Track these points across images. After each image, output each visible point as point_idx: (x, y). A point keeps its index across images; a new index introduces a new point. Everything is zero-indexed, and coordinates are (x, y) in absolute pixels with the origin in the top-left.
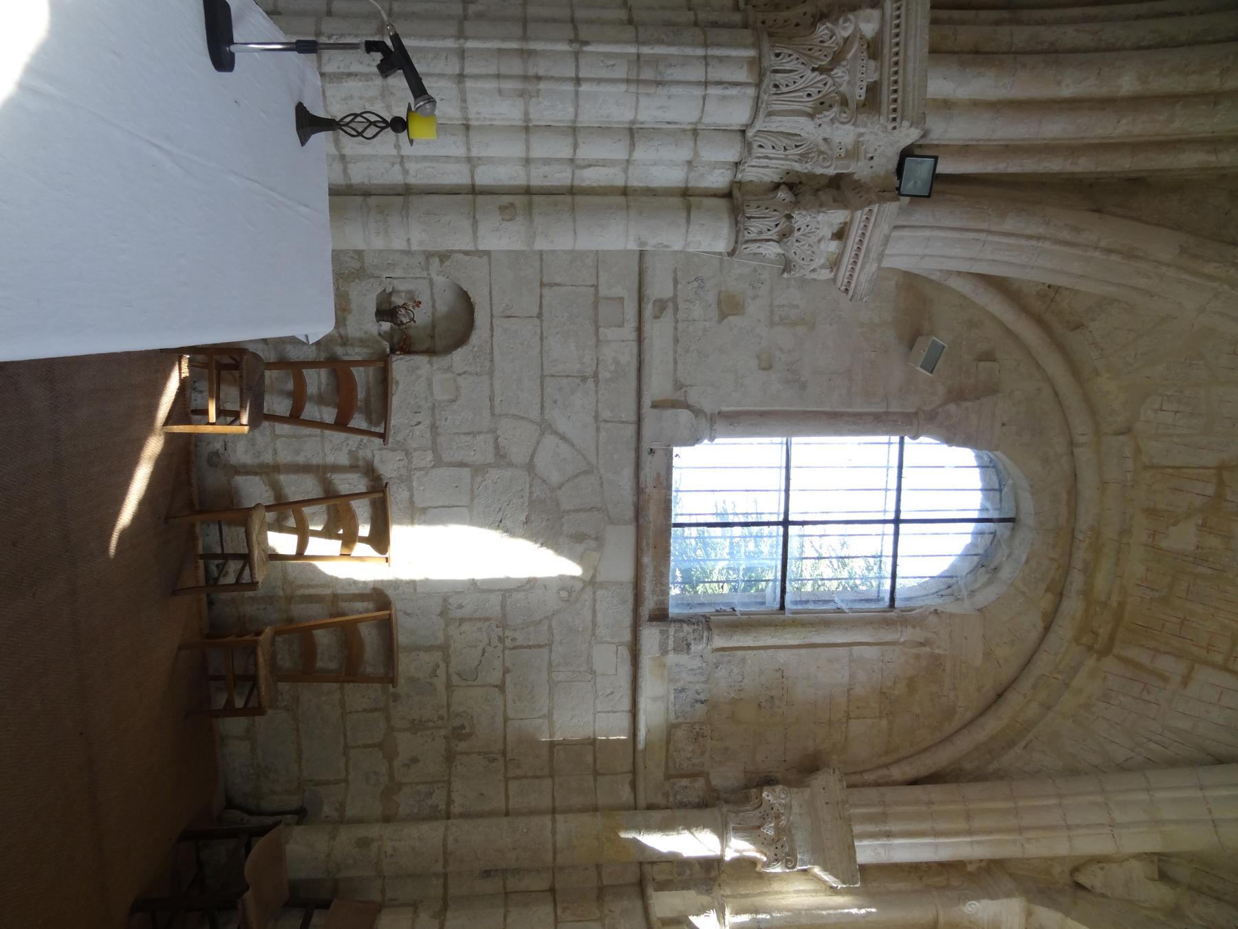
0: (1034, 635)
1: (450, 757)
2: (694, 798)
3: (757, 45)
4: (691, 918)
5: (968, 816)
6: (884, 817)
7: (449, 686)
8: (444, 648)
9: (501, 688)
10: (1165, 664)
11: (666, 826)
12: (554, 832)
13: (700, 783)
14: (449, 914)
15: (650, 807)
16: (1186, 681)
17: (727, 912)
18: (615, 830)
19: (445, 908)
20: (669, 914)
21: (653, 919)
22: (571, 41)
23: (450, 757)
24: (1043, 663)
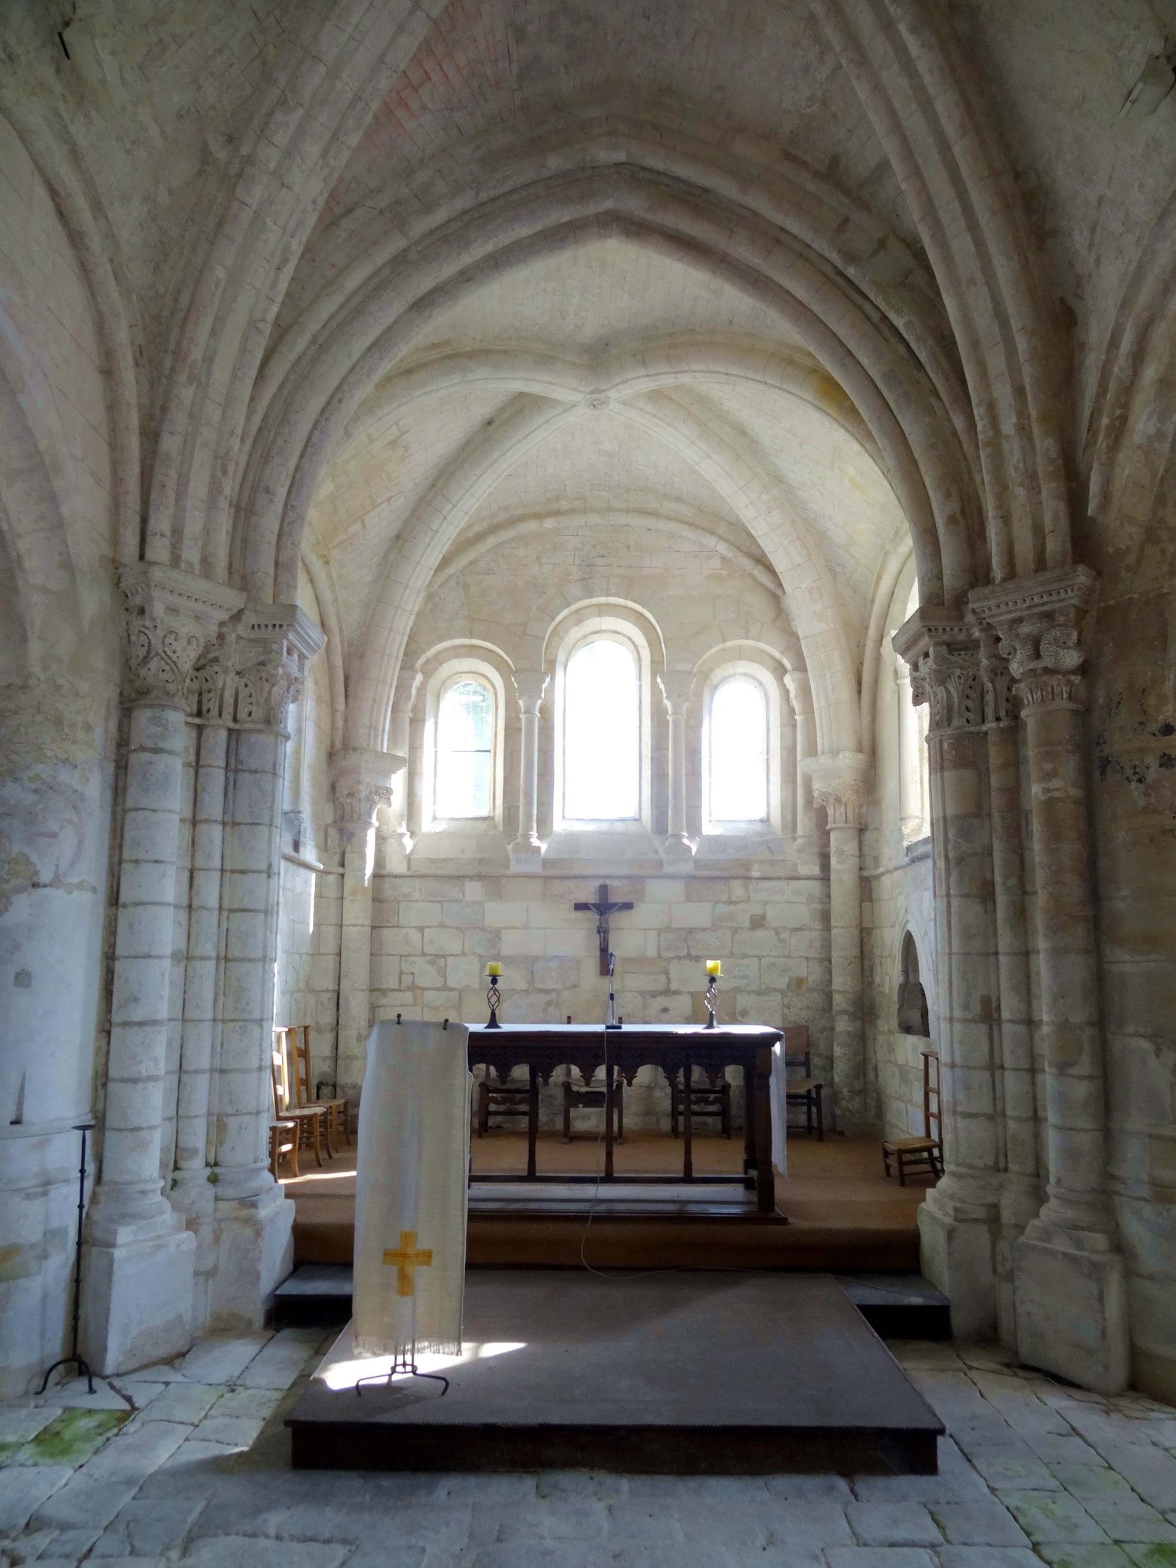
0: (311, 591)
1: (312, 991)
2: (338, 836)
3: (277, 735)
4: (408, 852)
5: (385, 683)
6: (376, 729)
7: (298, 991)
8: (292, 993)
9: (301, 955)
10: (352, 529)
11: (362, 857)
12: (363, 925)
13: (331, 831)
14: (384, 986)
15: (343, 865)
16: (364, 526)
17: (400, 831)
18: (364, 889)
19: (379, 990)
20: (405, 865)
21: (408, 873)
22: (269, 876)
23: (312, 991)
24: (327, 596)
